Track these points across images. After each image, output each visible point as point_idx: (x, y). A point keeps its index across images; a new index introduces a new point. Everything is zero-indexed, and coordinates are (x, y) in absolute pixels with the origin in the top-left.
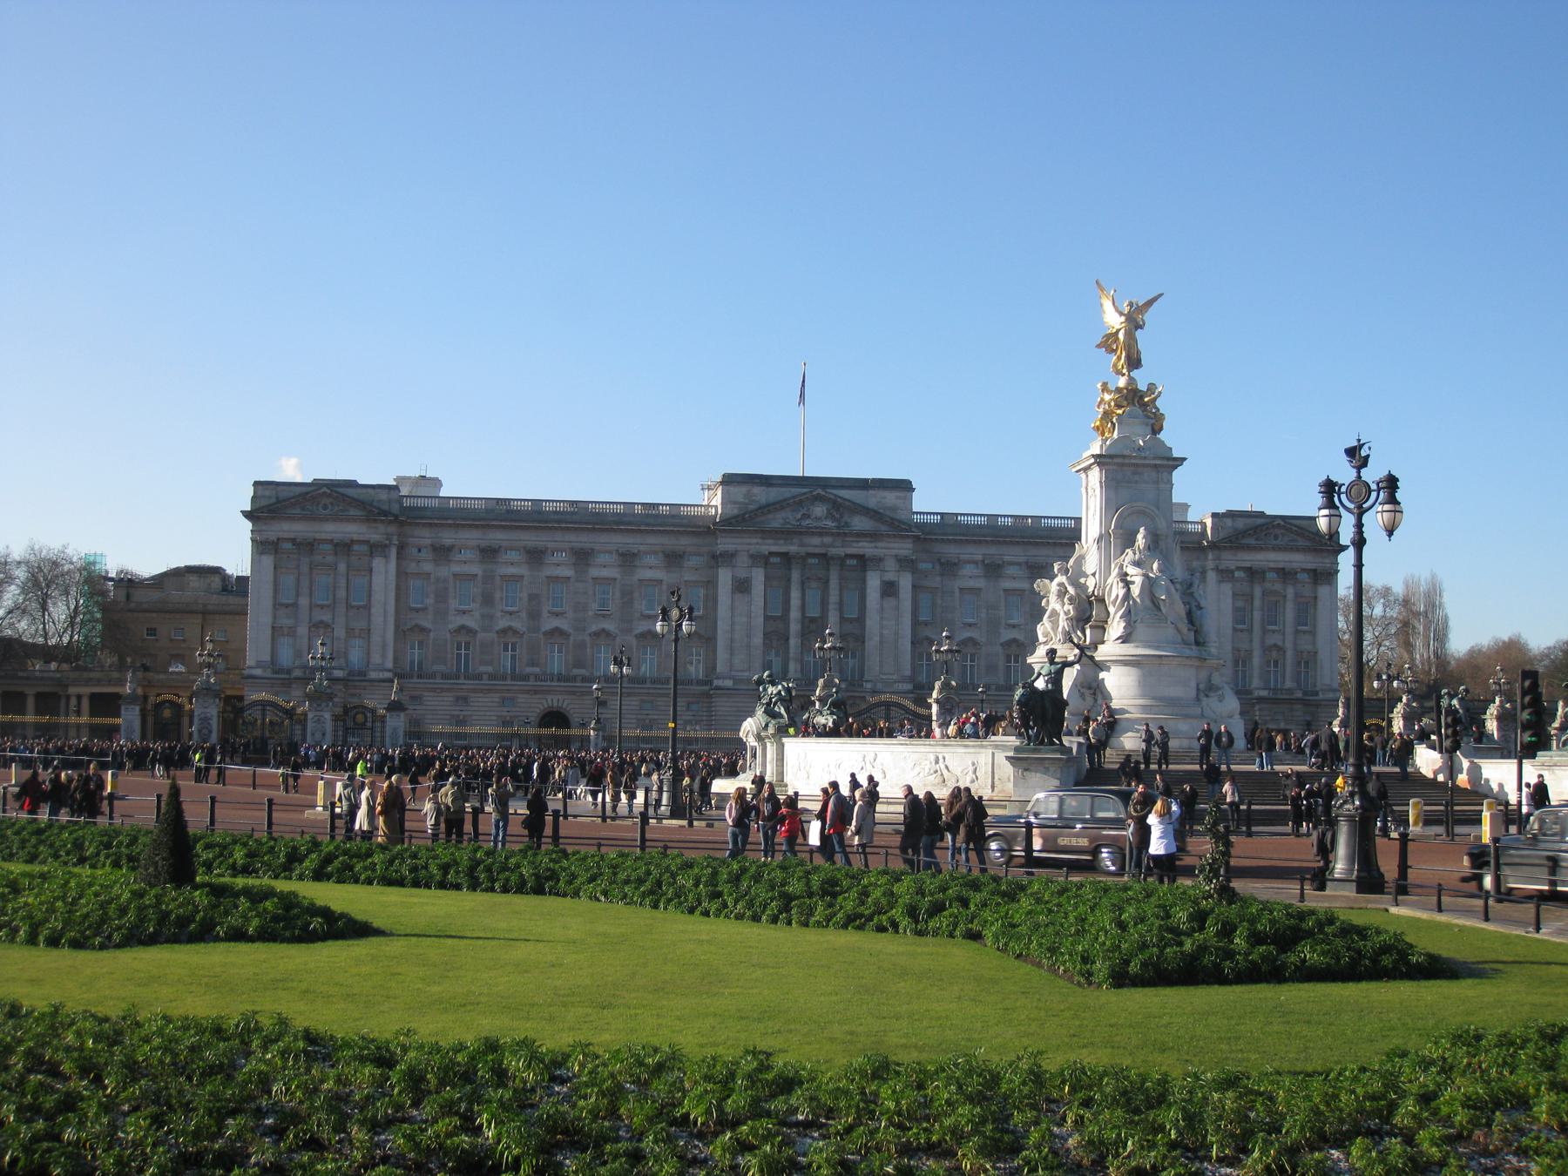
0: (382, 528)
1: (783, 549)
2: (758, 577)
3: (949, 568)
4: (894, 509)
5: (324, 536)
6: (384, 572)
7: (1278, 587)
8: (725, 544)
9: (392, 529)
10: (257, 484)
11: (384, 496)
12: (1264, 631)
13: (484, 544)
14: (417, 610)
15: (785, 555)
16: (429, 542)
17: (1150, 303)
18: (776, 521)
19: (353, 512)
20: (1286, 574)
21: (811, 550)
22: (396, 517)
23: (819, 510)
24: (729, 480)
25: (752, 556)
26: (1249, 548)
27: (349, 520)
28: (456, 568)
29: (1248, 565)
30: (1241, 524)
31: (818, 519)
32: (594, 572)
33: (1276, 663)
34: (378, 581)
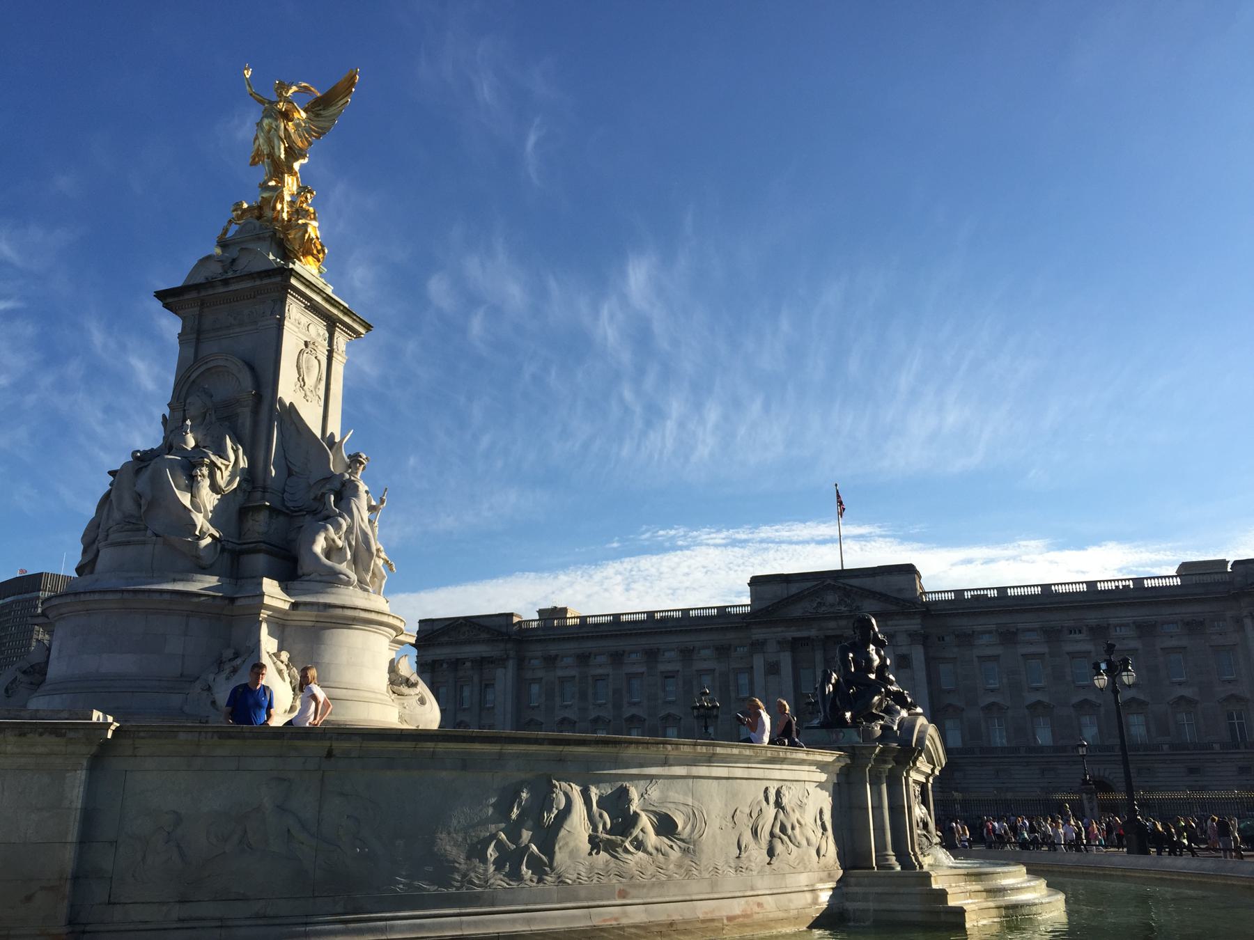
1: (804, 634)
2: (786, 659)
3: (966, 639)
4: (900, 590)
5: (463, 656)
6: (504, 678)
8: (758, 634)
10: (421, 622)
14: (533, 708)
15: (808, 638)
18: (797, 611)
19: (484, 636)
21: (829, 633)
23: (831, 598)
24: (756, 582)
25: (779, 642)
27: (478, 642)
28: (560, 673)
31: (832, 605)
32: (662, 667)
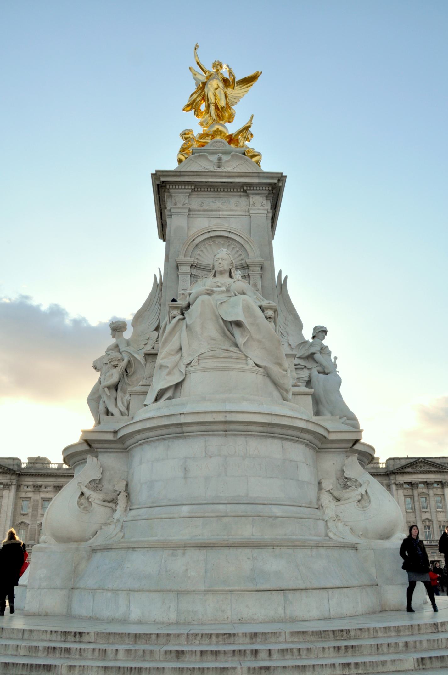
0: (9, 477)
7: (425, 491)
9: (14, 477)
11: (11, 462)
12: (421, 512)
13: (56, 484)
14: (24, 515)
16: (31, 483)
17: (249, 81)
20: (427, 484)
22: (15, 471)
26: (409, 473)
28: (43, 495)
29: (409, 481)
30: (404, 463)
33: (429, 527)
34: (5, 501)
